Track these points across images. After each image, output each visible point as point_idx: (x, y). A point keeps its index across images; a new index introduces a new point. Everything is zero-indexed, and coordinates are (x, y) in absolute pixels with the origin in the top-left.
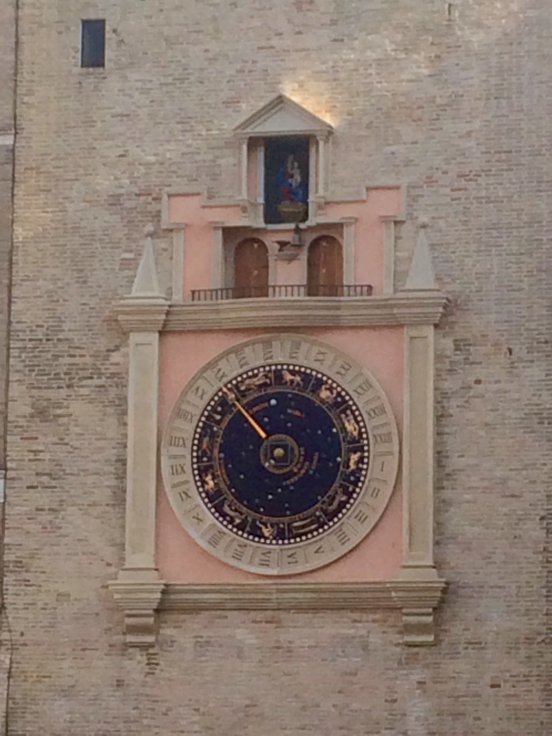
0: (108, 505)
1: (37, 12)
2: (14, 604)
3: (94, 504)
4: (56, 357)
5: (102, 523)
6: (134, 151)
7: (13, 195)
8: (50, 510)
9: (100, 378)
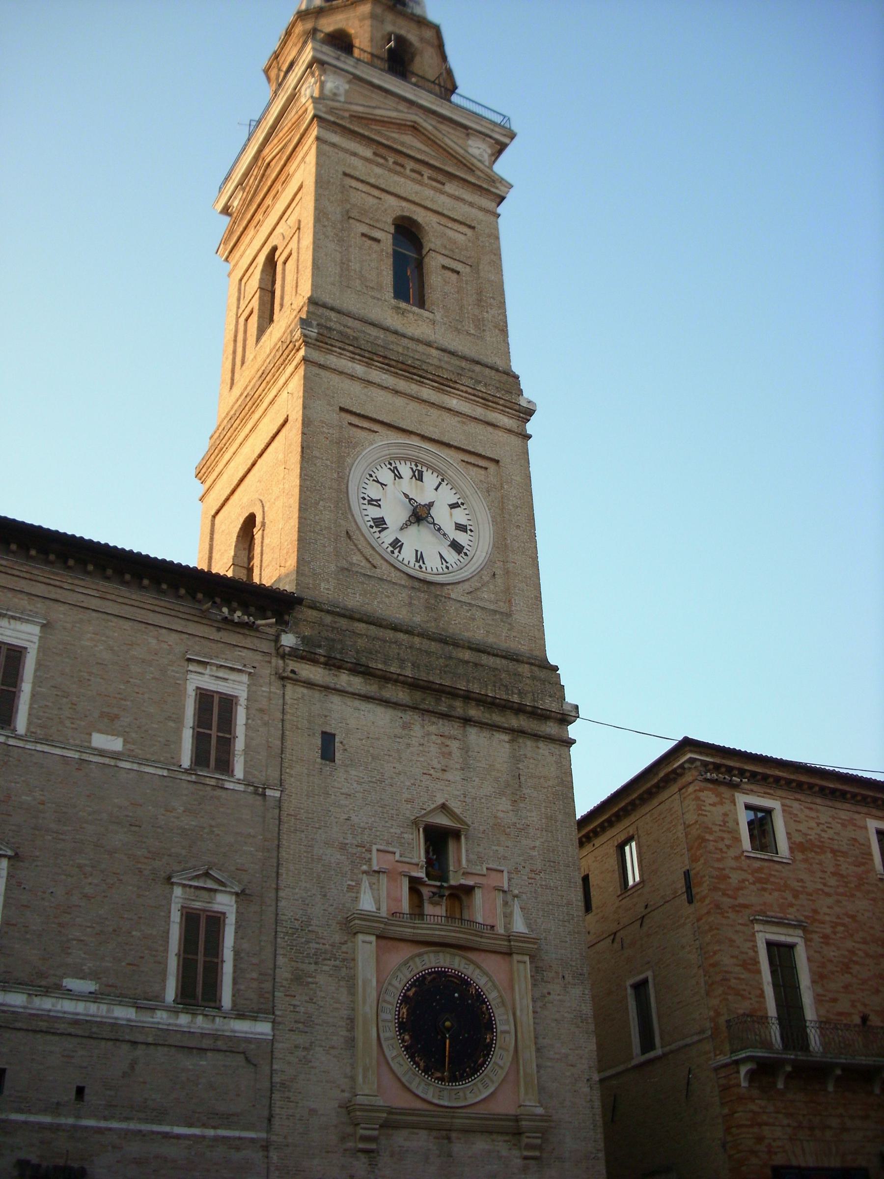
0: (342, 1049)
1: (295, 719)
2: (279, 1114)
3: (333, 1048)
4: (308, 942)
5: (338, 1061)
6: (353, 818)
7: (279, 830)
8: (303, 1048)
9: (335, 961)
